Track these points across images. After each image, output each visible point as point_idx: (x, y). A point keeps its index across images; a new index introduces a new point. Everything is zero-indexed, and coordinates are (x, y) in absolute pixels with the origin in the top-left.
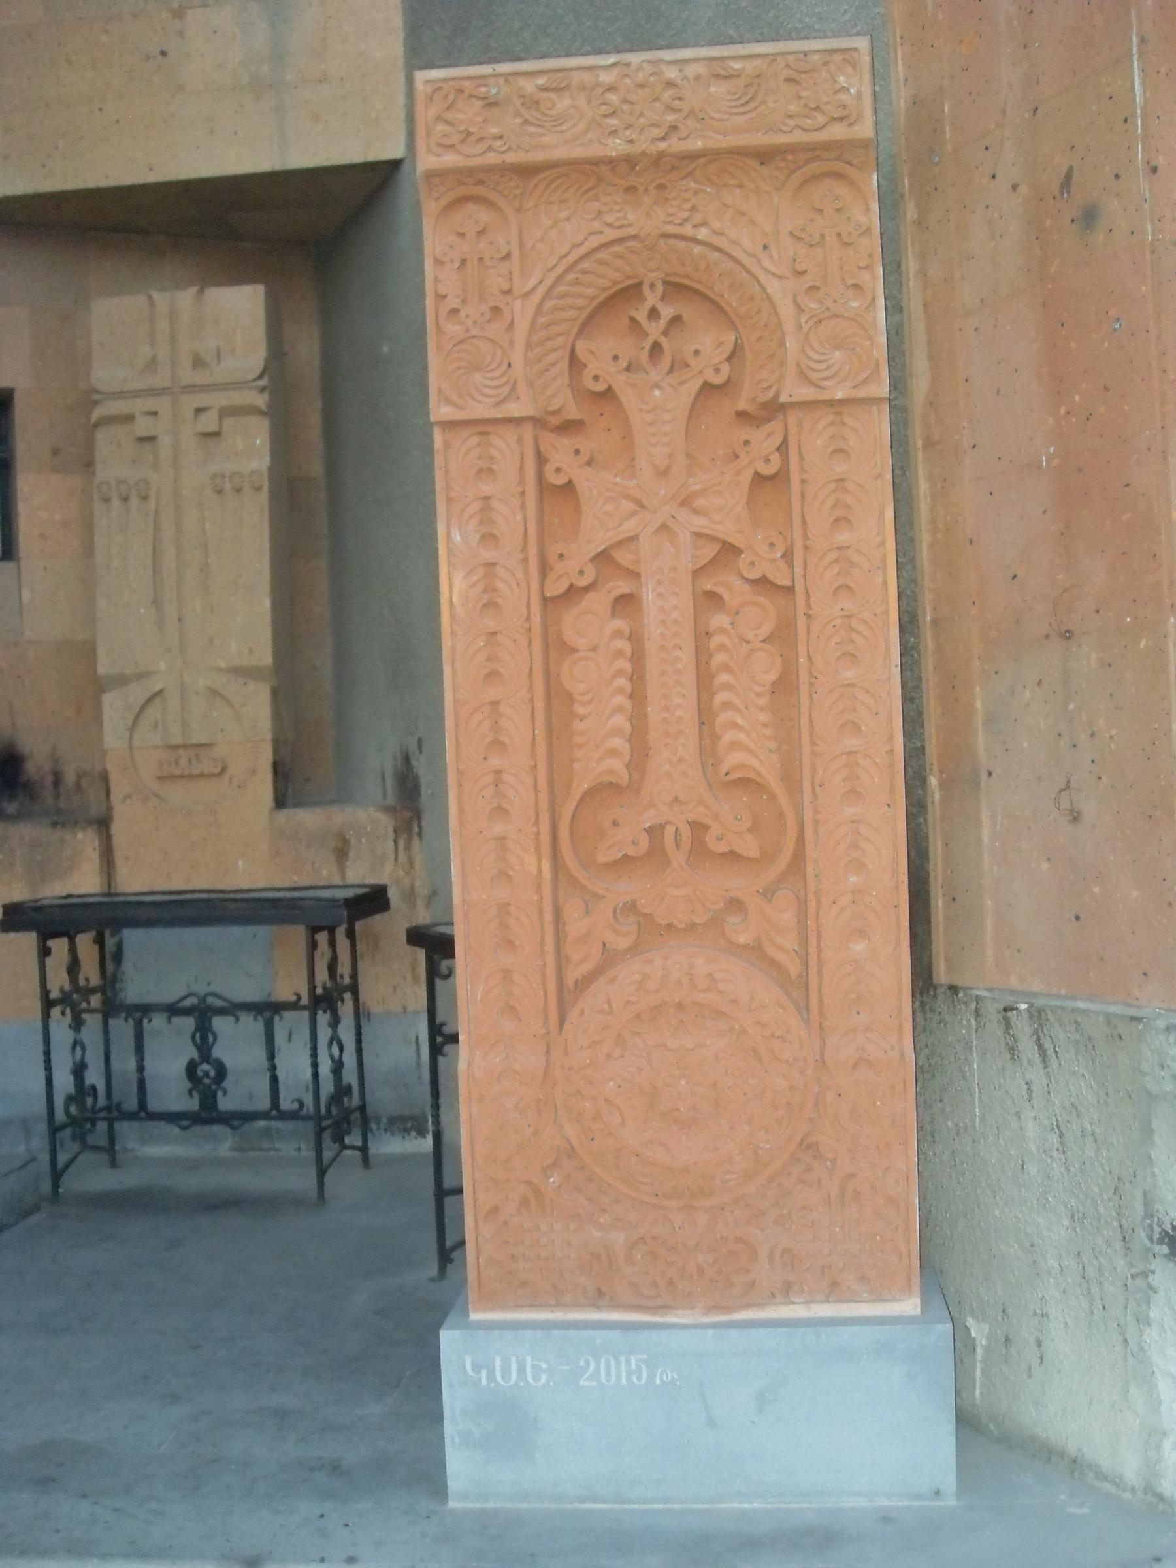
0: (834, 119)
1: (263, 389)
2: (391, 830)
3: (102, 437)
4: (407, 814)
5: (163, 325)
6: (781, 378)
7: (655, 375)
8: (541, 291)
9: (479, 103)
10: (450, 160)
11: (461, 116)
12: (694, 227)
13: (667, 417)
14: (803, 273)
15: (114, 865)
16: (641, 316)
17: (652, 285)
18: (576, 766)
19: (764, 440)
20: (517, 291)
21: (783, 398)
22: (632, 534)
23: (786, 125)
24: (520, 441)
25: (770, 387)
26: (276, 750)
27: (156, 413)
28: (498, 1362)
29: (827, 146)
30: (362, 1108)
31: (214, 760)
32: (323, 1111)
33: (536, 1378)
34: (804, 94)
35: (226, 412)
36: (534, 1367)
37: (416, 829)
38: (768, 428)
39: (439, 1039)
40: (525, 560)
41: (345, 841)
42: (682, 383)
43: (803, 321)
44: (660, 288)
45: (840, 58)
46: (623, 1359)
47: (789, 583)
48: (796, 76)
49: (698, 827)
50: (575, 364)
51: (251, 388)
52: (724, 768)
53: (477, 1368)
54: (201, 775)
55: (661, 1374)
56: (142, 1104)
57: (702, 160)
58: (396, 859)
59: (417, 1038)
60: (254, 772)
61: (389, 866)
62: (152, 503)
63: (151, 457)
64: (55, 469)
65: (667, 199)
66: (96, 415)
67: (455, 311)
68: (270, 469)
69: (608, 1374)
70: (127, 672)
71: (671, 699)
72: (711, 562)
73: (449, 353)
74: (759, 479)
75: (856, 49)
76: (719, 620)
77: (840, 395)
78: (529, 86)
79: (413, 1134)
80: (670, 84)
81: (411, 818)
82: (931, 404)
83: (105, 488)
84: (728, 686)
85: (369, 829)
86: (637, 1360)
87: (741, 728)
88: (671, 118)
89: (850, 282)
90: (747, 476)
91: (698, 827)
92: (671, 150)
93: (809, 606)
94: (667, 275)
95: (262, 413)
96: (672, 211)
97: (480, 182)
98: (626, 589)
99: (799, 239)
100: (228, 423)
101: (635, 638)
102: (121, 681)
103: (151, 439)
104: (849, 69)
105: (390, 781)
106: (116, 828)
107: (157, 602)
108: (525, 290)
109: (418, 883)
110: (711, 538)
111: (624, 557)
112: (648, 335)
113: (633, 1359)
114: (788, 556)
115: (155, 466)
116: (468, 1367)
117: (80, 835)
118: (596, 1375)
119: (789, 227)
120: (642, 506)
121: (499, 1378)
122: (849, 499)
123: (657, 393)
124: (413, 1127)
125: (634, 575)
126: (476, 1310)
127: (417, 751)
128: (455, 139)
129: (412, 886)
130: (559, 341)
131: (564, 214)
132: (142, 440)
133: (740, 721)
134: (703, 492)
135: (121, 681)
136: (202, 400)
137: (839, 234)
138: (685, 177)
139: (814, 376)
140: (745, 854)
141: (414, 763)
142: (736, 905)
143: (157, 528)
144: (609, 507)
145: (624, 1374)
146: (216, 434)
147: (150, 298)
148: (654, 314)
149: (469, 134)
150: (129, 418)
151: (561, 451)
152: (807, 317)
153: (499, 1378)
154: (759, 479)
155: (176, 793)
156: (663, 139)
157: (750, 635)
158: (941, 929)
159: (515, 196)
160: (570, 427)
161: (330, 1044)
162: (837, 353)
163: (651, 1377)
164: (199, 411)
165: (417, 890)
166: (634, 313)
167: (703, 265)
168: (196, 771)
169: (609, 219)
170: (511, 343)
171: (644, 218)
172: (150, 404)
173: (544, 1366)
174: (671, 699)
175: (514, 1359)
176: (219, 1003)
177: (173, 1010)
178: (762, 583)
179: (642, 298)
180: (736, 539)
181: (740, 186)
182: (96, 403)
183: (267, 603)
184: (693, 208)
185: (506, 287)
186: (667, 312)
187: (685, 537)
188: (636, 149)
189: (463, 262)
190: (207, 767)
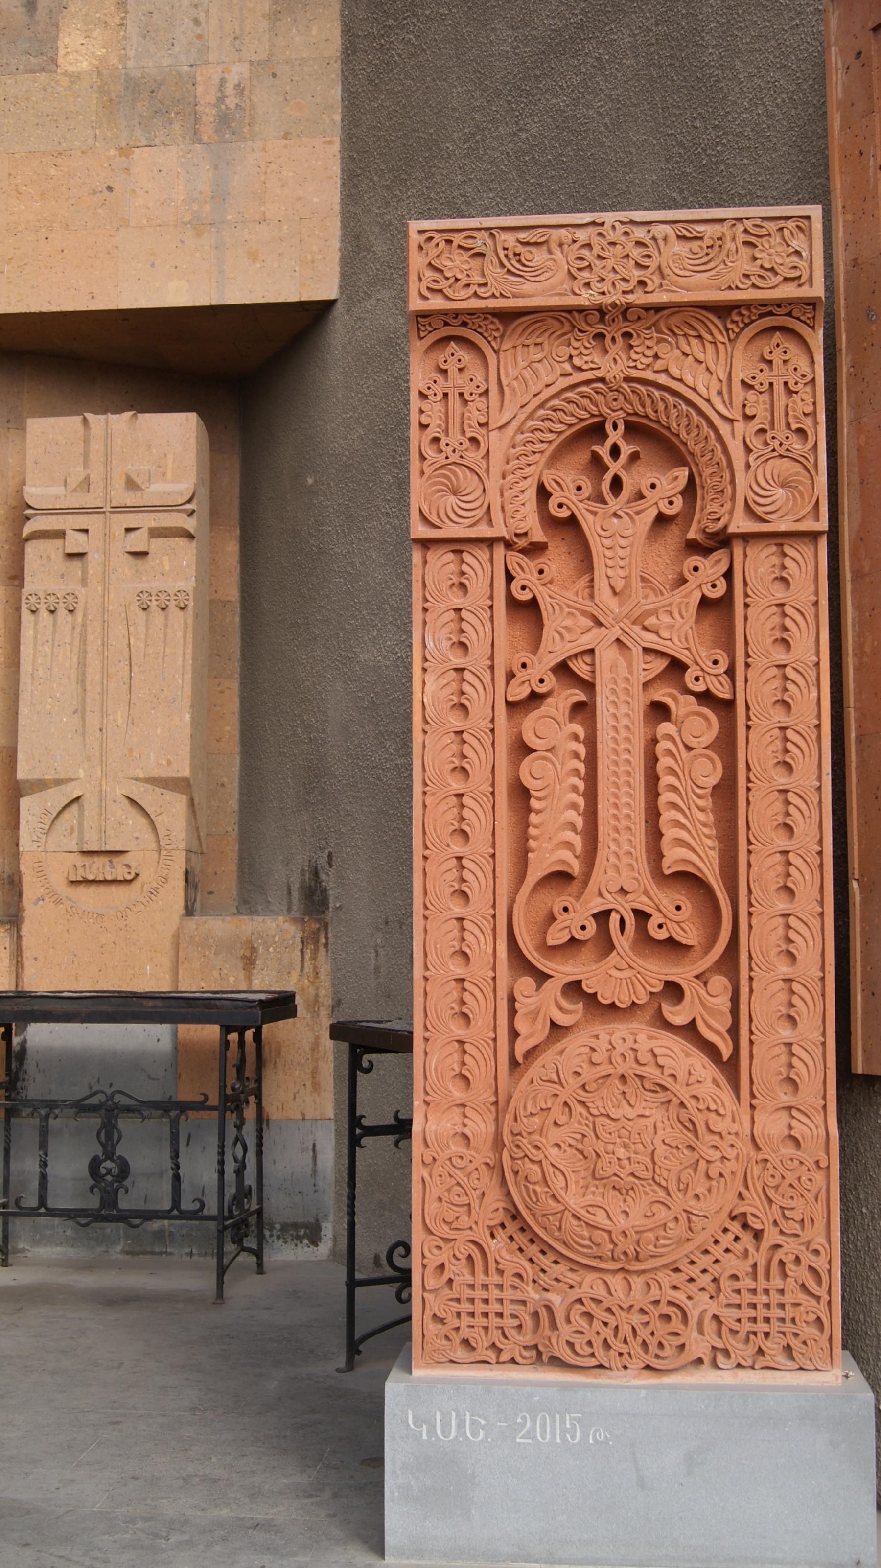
0: (786, 279)
1: (191, 513)
2: (298, 940)
3: (32, 550)
4: (315, 926)
5: (96, 447)
6: (731, 512)
7: (614, 504)
8: (515, 424)
9: (466, 255)
10: (437, 303)
11: (448, 263)
12: (655, 372)
13: (623, 542)
14: (754, 417)
15: (22, 967)
16: (604, 452)
17: (615, 427)
18: (530, 855)
19: (711, 568)
20: (492, 426)
21: (732, 529)
22: (589, 647)
23: (743, 283)
24: (491, 560)
25: (719, 519)
26: (188, 860)
27: (86, 531)
28: (438, 1417)
29: (778, 303)
30: (260, 1212)
31: (128, 866)
32: (226, 1213)
33: (475, 1434)
34: (758, 255)
35: (156, 533)
36: (473, 1422)
37: (323, 941)
38: (715, 556)
39: (358, 1131)
40: (492, 668)
41: (254, 950)
42: (638, 513)
43: (751, 459)
44: (621, 427)
45: (794, 224)
46: (558, 1416)
47: (727, 696)
48: (752, 239)
49: (642, 916)
50: (543, 494)
52: (666, 862)
53: (418, 1422)
54: (114, 882)
55: (595, 1432)
56: (42, 1201)
57: (666, 312)
58: (302, 970)
59: (314, 1145)
60: (166, 879)
61: (295, 975)
63: (80, 573)
65: (631, 347)
66: (27, 530)
67: (436, 440)
68: (196, 589)
69: (544, 1431)
70: (46, 777)
71: (620, 798)
72: (659, 677)
73: (429, 478)
74: (705, 602)
75: (808, 218)
76: (665, 728)
77: (783, 528)
78: (509, 239)
79: (306, 1241)
80: (639, 244)
81: (319, 929)
82: (861, 539)
83: (33, 599)
84: (673, 788)
85: (277, 939)
86: (571, 1418)
87: (682, 826)
88: (637, 274)
89: (794, 426)
90: (696, 597)
91: (642, 916)
92: (638, 302)
93: (748, 718)
94: (629, 414)
95: (191, 537)
96: (634, 357)
97: (464, 324)
98: (582, 697)
99: (751, 387)
100: (156, 545)
101: (591, 743)
102: (41, 785)
103: (81, 555)
104: (801, 235)
105: (295, 894)
106: (25, 930)
107: (81, 712)
108: (500, 424)
109: (322, 992)
110: (663, 654)
111: (580, 668)
112: (608, 468)
113: (568, 1417)
114: (731, 672)
115: (84, 582)
116: (410, 1421)
118: (530, 1434)
119: (741, 376)
120: (600, 624)
121: (439, 1433)
122: (788, 622)
123: (615, 521)
124: (305, 1236)
125: (589, 686)
126: (419, 1367)
127: (327, 866)
128: (443, 284)
129: (317, 995)
130: (528, 471)
131: (539, 357)
132: (71, 556)
133: (683, 820)
134: (654, 612)
135: (41, 785)
136: (132, 520)
137: (786, 383)
138: (648, 328)
139: (759, 510)
140: (684, 941)
141: (323, 877)
142: (674, 991)
143: (84, 641)
144: (568, 622)
145: (558, 1432)
146: (144, 554)
147: (85, 421)
148: (615, 452)
149: (457, 280)
150: (60, 534)
151: (526, 572)
152: (756, 455)
153: (439, 1433)
154: (705, 602)
155: (87, 897)
156: (631, 292)
157: (693, 742)
158: (859, 1022)
159: (495, 338)
160: (535, 549)
161: (235, 1144)
162: (781, 490)
163: (585, 1436)
164: (128, 530)
165: (320, 1000)
166: (596, 448)
167: (661, 406)
168: (109, 878)
169: (577, 361)
170: (488, 470)
171: (612, 364)
172: (82, 521)
173: (483, 1422)
174: (620, 798)
175: (454, 1414)
176: (125, 1101)
177: (81, 1107)
178: (706, 697)
179: (605, 436)
180: (684, 656)
181: (700, 337)
183: (188, 717)
184: (656, 357)
185: (483, 420)
186: (626, 450)
187: (637, 651)
188: (607, 300)
189: (446, 395)
190: (121, 873)
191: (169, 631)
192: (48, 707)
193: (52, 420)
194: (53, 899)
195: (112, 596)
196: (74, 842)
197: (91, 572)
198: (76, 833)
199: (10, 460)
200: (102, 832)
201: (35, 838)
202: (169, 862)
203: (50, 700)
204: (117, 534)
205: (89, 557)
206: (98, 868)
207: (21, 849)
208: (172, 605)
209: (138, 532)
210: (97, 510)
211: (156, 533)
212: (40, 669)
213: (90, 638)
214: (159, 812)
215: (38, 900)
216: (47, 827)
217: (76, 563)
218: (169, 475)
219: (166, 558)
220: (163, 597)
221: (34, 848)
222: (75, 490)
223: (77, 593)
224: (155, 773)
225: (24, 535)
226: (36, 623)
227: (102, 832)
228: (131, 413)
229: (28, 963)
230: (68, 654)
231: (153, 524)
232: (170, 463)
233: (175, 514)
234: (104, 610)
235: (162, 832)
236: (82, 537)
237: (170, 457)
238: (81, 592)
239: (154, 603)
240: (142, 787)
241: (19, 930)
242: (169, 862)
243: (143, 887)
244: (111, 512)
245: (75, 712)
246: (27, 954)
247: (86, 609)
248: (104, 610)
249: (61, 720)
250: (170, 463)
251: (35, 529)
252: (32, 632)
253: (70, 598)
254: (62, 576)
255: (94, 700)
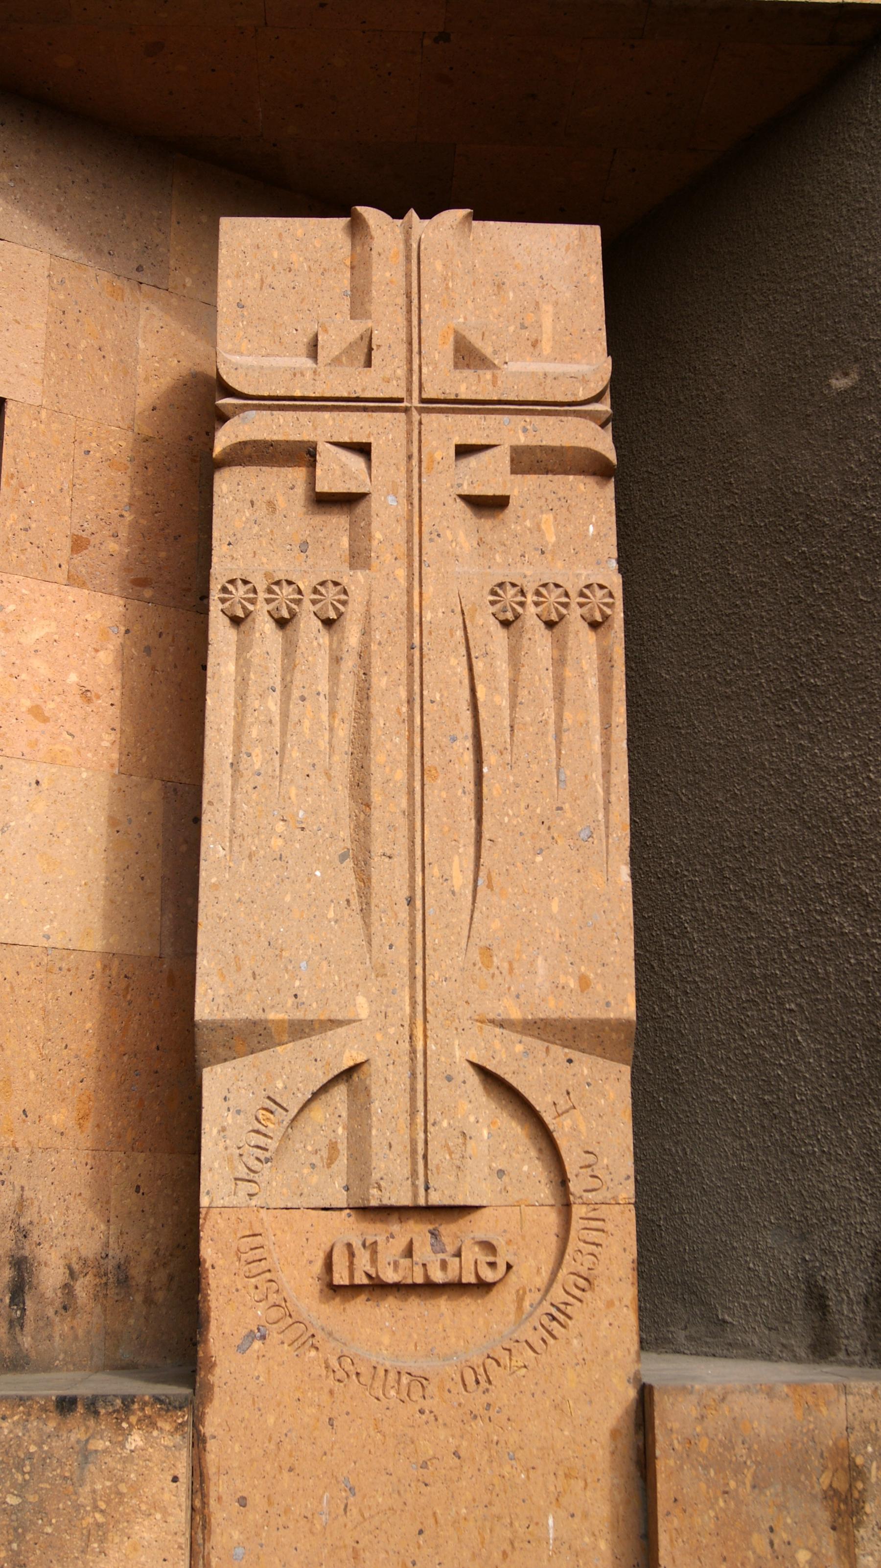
3: (228, 487)
5: (387, 274)
15: (206, 1525)
27: (363, 450)
31: (489, 1247)
35: (527, 461)
51: (577, 414)
62: (352, 636)
63: (345, 542)
64: (73, 580)
66: (224, 439)
70: (272, 1016)
83: (240, 592)
100: (520, 488)
102: (253, 1037)
103: (348, 501)
115: (359, 557)
117: (136, 1440)
135: (253, 1037)
143: (364, 693)
155: (375, 1329)
164: (463, 451)
172: (355, 425)
182: (222, 418)
183: (624, 874)
191: (569, 673)
192: (277, 843)
193: (279, 222)
194: (291, 1335)
195: (429, 590)
196: (339, 1183)
197: (378, 535)
198: (343, 1160)
199: (141, 345)
200: (420, 1157)
201: (243, 1172)
202: (593, 1236)
203: (280, 827)
204: (438, 456)
205: (375, 503)
206: (392, 1252)
207: (204, 1201)
208: (575, 614)
209: (485, 456)
210: (387, 404)
211: (527, 461)
212: (257, 751)
213: (379, 682)
214: (563, 1104)
215: (251, 1337)
216: (272, 1145)
217: (337, 523)
218: (546, 347)
219: (547, 518)
220: (554, 596)
221: (241, 1198)
222: (336, 361)
223: (345, 581)
224: (552, 1008)
225: (218, 449)
226: (242, 648)
227: (420, 1157)
228: (462, 213)
229: (220, 1514)
230: (324, 717)
231: (522, 440)
232: (547, 322)
233: (572, 422)
234: (414, 620)
235: (572, 1160)
236: (355, 462)
237: (548, 309)
238: (357, 581)
239: (532, 609)
240: (519, 1044)
241: (198, 1421)
242: (593, 1236)
243: (520, 1300)
244: (421, 411)
245: (343, 858)
246: (219, 1487)
247: (368, 617)
248: (414, 620)
249: (311, 874)
250: (547, 322)
251: (243, 438)
252: (232, 667)
253: (331, 593)
254: (304, 547)
255: (392, 827)
